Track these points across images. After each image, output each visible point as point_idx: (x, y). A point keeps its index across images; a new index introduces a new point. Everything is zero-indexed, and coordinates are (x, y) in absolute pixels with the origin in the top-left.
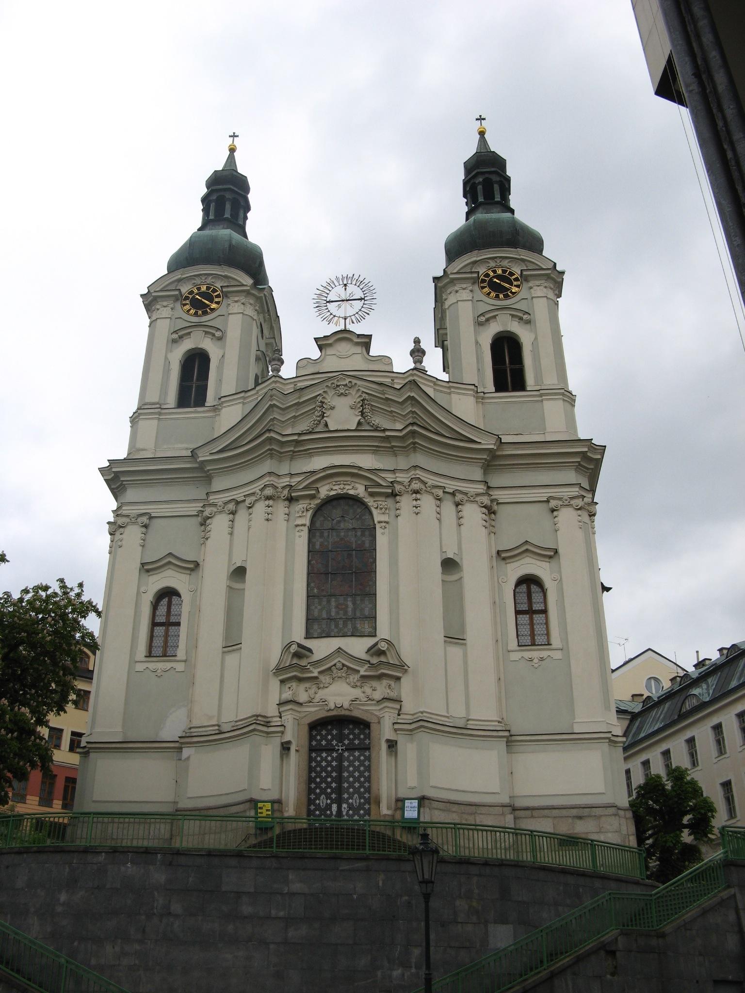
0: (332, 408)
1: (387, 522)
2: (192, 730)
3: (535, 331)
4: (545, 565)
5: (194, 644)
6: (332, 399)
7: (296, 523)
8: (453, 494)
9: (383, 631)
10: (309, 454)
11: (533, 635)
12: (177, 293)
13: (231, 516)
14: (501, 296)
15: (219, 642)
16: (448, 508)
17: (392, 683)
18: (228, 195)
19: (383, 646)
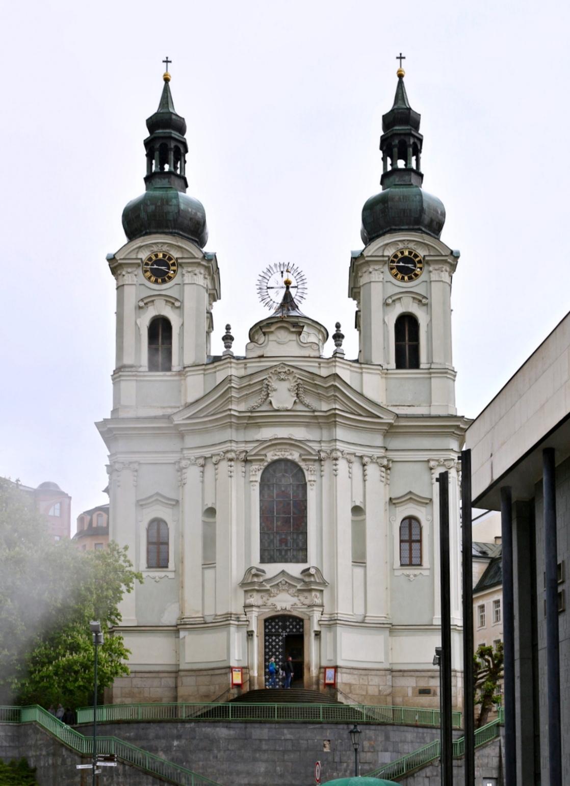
0: (275, 390)
1: (314, 481)
2: (185, 620)
3: (429, 313)
5: (181, 561)
6: (274, 384)
7: (251, 479)
8: (361, 457)
9: (313, 560)
10: (259, 426)
11: (411, 557)
12: (139, 261)
13: (201, 469)
14: (406, 278)
15: (199, 561)
16: (357, 468)
17: (318, 594)
18: (173, 144)
19: (312, 571)
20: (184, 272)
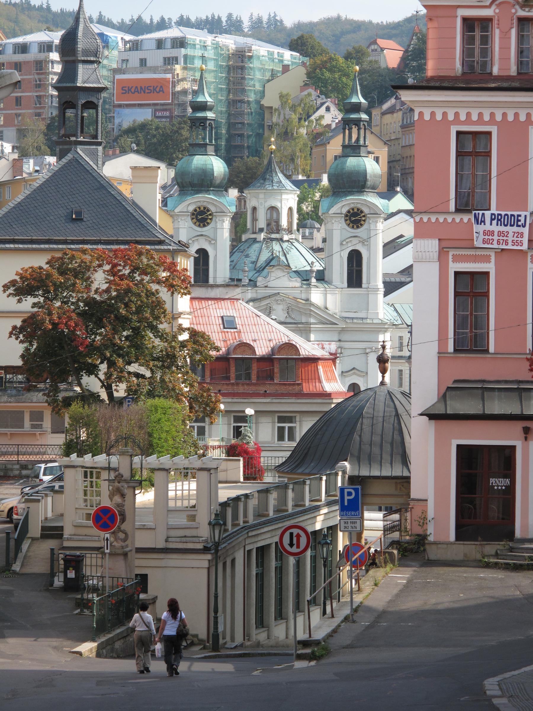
4: (362, 379)
6: (274, 307)
20: (217, 220)
